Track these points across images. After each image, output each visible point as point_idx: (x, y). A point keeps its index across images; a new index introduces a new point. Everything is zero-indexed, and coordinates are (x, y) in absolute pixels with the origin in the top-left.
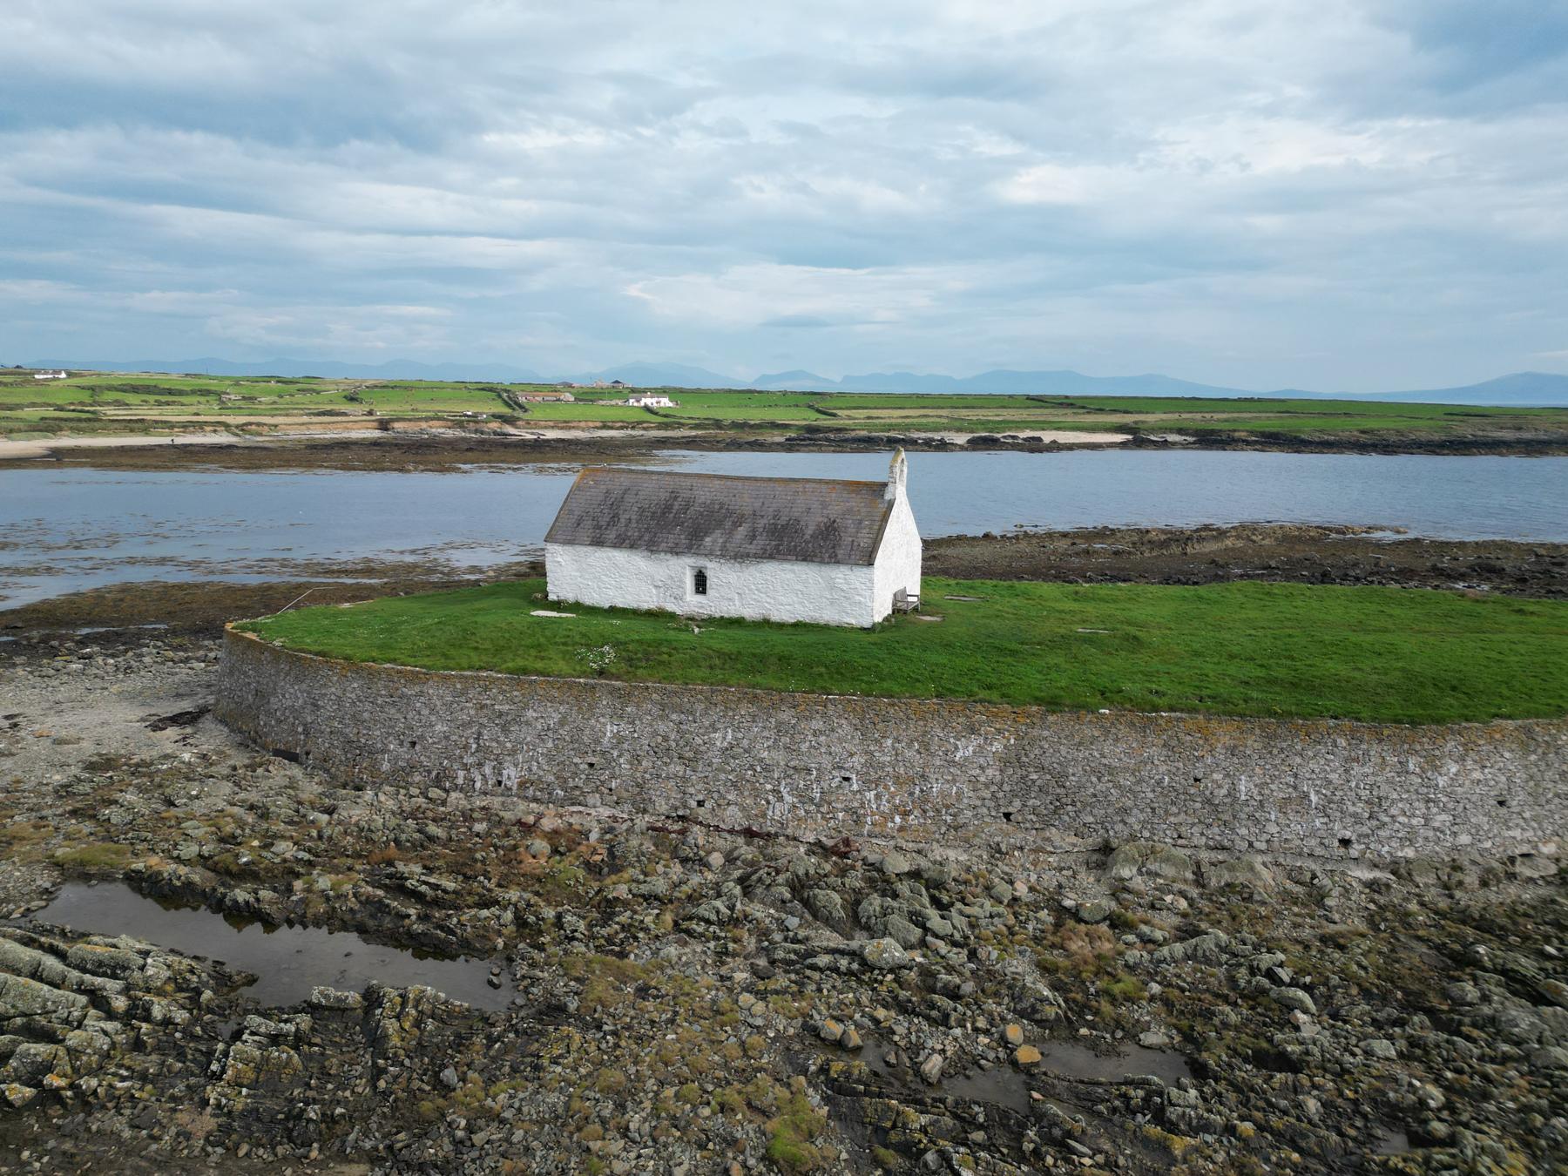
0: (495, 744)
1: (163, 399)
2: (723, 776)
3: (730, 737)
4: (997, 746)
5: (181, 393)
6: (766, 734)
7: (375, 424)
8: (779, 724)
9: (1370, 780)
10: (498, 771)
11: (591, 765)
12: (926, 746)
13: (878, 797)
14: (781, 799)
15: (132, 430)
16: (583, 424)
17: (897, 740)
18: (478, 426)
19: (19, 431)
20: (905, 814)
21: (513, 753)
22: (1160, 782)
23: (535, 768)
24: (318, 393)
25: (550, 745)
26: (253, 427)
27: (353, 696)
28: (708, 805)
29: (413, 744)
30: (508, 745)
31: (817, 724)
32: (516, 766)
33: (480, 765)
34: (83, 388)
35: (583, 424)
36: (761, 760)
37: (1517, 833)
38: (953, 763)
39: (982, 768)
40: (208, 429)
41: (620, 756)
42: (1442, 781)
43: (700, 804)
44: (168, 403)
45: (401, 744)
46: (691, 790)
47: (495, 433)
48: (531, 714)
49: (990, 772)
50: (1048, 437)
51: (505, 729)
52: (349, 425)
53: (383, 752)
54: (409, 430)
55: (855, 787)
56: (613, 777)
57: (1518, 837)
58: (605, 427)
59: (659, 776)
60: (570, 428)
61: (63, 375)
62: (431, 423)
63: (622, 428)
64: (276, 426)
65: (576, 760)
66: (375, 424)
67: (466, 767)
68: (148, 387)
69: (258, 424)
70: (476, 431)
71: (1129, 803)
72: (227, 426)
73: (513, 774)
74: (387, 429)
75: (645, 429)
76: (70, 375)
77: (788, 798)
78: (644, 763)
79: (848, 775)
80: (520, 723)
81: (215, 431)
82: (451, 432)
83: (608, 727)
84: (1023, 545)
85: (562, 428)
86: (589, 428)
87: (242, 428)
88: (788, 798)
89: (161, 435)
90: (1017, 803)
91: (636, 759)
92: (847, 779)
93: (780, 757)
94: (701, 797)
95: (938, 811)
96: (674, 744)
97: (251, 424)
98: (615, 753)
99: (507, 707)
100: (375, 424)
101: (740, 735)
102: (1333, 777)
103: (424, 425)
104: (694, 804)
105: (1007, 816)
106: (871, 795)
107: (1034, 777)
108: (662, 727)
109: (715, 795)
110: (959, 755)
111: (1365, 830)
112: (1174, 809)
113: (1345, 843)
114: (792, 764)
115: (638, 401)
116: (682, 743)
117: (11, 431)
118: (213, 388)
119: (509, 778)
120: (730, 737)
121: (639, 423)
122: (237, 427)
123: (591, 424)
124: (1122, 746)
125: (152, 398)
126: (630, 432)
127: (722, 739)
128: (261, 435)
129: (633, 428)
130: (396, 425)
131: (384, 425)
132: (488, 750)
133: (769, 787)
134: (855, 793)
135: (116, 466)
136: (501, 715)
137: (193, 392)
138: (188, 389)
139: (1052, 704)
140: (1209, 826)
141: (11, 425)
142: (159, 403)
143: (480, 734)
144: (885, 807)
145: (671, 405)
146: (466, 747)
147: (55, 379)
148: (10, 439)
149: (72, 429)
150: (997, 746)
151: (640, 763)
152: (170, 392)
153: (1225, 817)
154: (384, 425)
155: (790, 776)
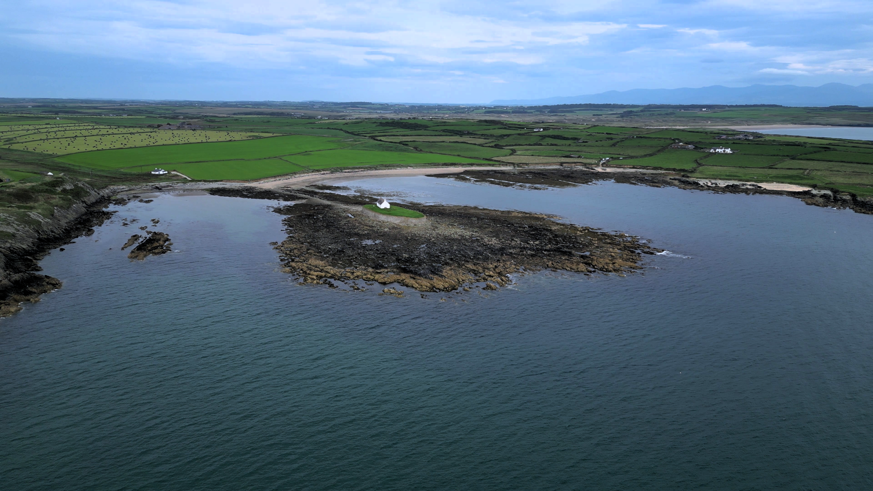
34: (540, 136)
35: (626, 166)
50: (765, 186)
61: (542, 130)
62: (577, 164)
63: (639, 168)
66: (560, 164)
70: (588, 168)
74: (561, 165)
75: (648, 169)
76: (544, 129)
100: (560, 164)
115: (715, 150)
117: (464, 165)
123: (629, 167)
128: (521, 167)
130: (564, 165)
138: (570, 137)
145: (731, 152)
147: (539, 131)
154: (561, 164)
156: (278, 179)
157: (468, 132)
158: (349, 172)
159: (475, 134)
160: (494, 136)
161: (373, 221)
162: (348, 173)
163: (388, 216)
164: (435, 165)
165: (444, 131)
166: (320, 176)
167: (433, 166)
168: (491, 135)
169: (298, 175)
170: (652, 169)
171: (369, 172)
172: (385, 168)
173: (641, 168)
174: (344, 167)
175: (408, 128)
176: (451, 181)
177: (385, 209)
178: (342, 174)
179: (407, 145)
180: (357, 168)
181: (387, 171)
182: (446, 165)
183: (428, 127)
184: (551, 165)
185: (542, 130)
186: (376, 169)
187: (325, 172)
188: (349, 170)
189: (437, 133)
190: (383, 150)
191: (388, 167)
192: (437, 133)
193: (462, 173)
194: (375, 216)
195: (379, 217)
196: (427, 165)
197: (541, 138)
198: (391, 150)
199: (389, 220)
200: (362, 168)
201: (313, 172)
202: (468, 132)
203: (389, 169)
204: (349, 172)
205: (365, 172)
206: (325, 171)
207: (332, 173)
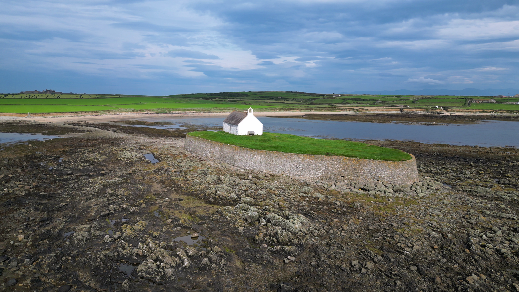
1: (359, 102)
5: (366, 100)
7: (399, 109)
15: (329, 110)
16: (474, 111)
18: (433, 111)
19: (303, 110)
24: (405, 100)
26: (361, 110)
34: (342, 99)
35: (474, 111)
37: (262, 168)
40: (348, 110)
44: (359, 103)
47: (438, 113)
52: (391, 110)
54: (408, 112)
57: (263, 168)
58: (483, 112)
60: (469, 112)
61: (340, 96)
62: (417, 109)
63: (491, 112)
64: (368, 110)
68: (358, 99)
69: (362, 109)
70: (432, 112)
72: (353, 109)
74: (402, 111)
75: (501, 113)
76: (342, 95)
81: (350, 111)
82: (423, 112)
84: (471, 149)
85: (465, 112)
86: (476, 112)
87: (357, 110)
89: (336, 111)
97: (360, 109)
103: (414, 110)
117: (302, 110)
118: (375, 99)
121: (498, 110)
122: (357, 110)
123: (478, 111)
125: (356, 102)
126: (494, 114)
128: (362, 112)
129: (496, 112)
131: (401, 110)
135: (313, 119)
137: (370, 100)
138: (368, 99)
139: (225, 143)
141: (302, 108)
142: (357, 103)
148: (301, 112)
149: (315, 109)
152: (364, 100)
156: (80, 115)
157: (281, 97)
158: (178, 113)
159: (287, 99)
160: (303, 100)
161: (219, 173)
162: (177, 114)
163: (274, 155)
164: (272, 110)
165: (262, 97)
166: (141, 115)
167: (270, 111)
168: (301, 99)
169: (112, 113)
170: (507, 112)
171: (202, 113)
172: (220, 111)
173: (493, 112)
174: (173, 109)
175: (233, 96)
176: (300, 119)
177: (251, 136)
178: (170, 114)
179: (235, 102)
180: (187, 110)
181: (222, 113)
182: (284, 110)
183: (248, 95)
184: (390, 111)
185: (340, 96)
186: (209, 112)
187: (149, 112)
188: (179, 112)
189: (257, 98)
190: (215, 104)
191: (222, 110)
192: (255, 98)
193: (304, 116)
194: (222, 157)
195: (235, 160)
196: (264, 109)
197: (343, 100)
198: (222, 104)
199: (277, 170)
200: (194, 110)
201: (133, 111)
202: (281, 97)
203: (224, 112)
204: (178, 113)
205: (197, 114)
206: (150, 111)
207: (157, 113)
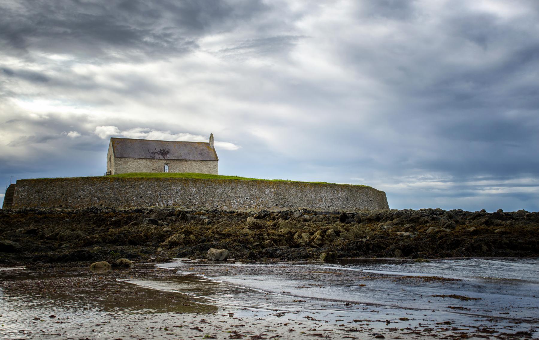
0: (165, 196)
2: (221, 200)
3: (221, 190)
4: (273, 190)
6: (229, 189)
8: (232, 187)
9: (330, 195)
10: (167, 202)
11: (190, 199)
12: (260, 190)
13: (254, 202)
14: (235, 204)
17: (255, 190)
20: (259, 206)
21: (170, 197)
22: (300, 197)
23: (176, 201)
25: (179, 195)
27: (117, 187)
28: (219, 206)
29: (141, 197)
30: (169, 195)
31: (239, 187)
32: (171, 200)
33: (162, 201)
36: (229, 195)
38: (266, 194)
39: (271, 195)
41: (197, 196)
42: (340, 195)
43: (217, 206)
45: (138, 197)
46: (215, 203)
48: (173, 187)
49: (273, 196)
51: (167, 192)
53: (132, 200)
55: (249, 200)
56: (196, 202)
59: (207, 201)
65: (186, 198)
67: (158, 202)
71: (296, 201)
73: (171, 202)
77: (236, 204)
78: (203, 198)
79: (246, 197)
80: (170, 190)
83: (193, 190)
88: (236, 204)
90: (278, 202)
91: (201, 197)
92: (247, 198)
93: (232, 194)
94: (217, 205)
95: (265, 204)
96: (209, 193)
98: (196, 196)
99: (166, 186)
101: (224, 190)
102: (325, 194)
104: (216, 207)
105: (277, 205)
106: (252, 202)
107: (280, 196)
108: (205, 189)
109: (220, 204)
110: (267, 192)
111: (331, 204)
112: (303, 202)
113: (329, 207)
114: (236, 196)
116: (211, 192)
119: (170, 204)
120: (221, 190)
124: (293, 190)
127: (220, 191)
132: (163, 197)
133: (232, 201)
134: (249, 201)
136: (165, 188)
140: (309, 205)
143: (160, 193)
144: (255, 204)
146: (157, 197)
150: (273, 190)
151: (202, 198)
153: (311, 203)
155: (236, 198)
